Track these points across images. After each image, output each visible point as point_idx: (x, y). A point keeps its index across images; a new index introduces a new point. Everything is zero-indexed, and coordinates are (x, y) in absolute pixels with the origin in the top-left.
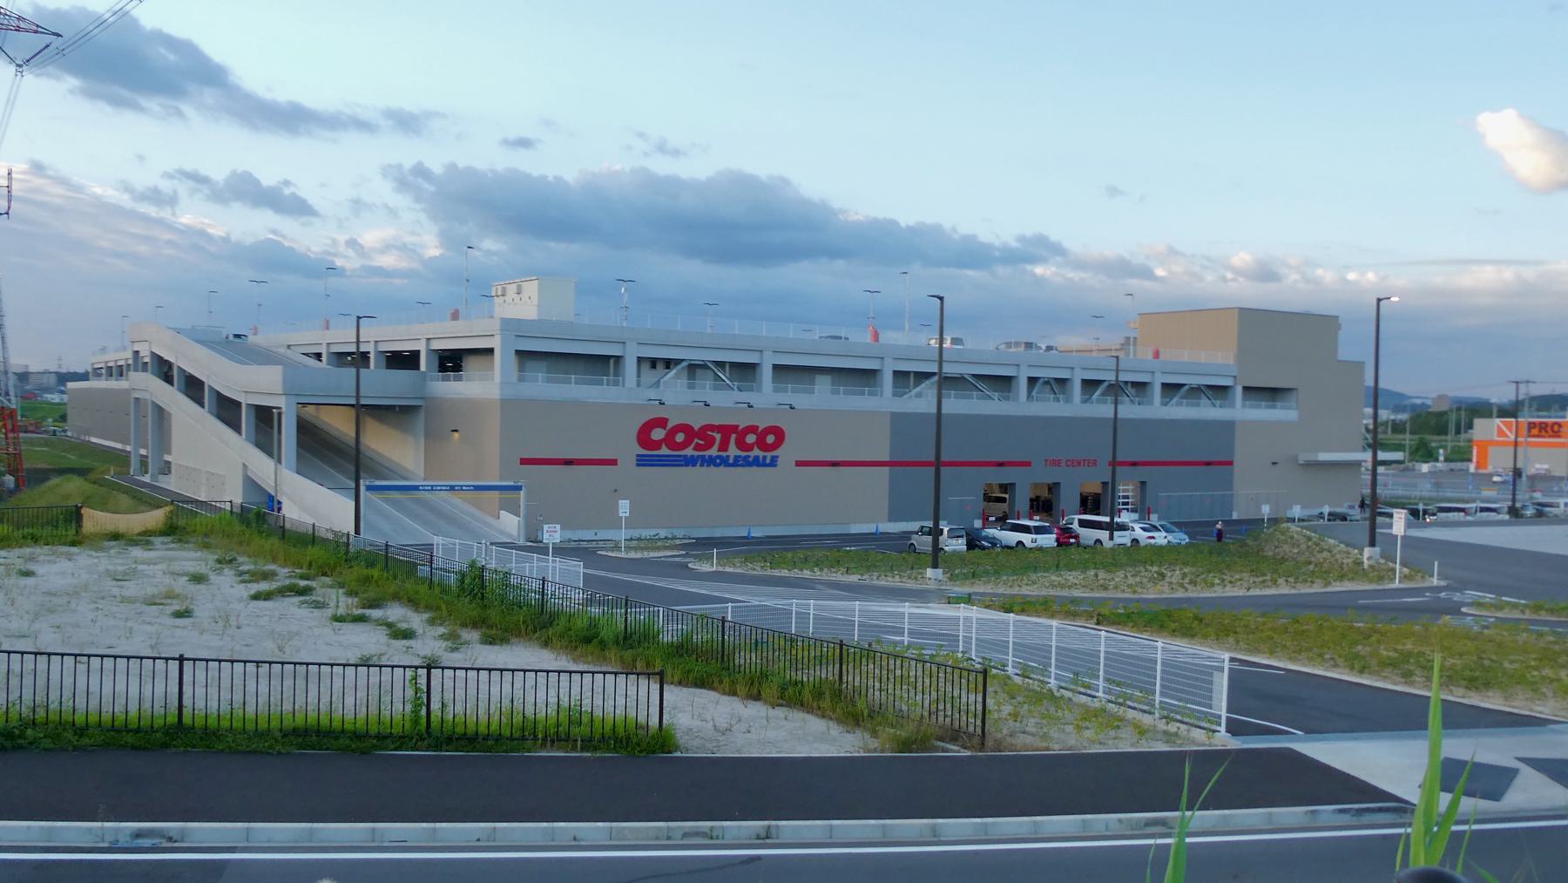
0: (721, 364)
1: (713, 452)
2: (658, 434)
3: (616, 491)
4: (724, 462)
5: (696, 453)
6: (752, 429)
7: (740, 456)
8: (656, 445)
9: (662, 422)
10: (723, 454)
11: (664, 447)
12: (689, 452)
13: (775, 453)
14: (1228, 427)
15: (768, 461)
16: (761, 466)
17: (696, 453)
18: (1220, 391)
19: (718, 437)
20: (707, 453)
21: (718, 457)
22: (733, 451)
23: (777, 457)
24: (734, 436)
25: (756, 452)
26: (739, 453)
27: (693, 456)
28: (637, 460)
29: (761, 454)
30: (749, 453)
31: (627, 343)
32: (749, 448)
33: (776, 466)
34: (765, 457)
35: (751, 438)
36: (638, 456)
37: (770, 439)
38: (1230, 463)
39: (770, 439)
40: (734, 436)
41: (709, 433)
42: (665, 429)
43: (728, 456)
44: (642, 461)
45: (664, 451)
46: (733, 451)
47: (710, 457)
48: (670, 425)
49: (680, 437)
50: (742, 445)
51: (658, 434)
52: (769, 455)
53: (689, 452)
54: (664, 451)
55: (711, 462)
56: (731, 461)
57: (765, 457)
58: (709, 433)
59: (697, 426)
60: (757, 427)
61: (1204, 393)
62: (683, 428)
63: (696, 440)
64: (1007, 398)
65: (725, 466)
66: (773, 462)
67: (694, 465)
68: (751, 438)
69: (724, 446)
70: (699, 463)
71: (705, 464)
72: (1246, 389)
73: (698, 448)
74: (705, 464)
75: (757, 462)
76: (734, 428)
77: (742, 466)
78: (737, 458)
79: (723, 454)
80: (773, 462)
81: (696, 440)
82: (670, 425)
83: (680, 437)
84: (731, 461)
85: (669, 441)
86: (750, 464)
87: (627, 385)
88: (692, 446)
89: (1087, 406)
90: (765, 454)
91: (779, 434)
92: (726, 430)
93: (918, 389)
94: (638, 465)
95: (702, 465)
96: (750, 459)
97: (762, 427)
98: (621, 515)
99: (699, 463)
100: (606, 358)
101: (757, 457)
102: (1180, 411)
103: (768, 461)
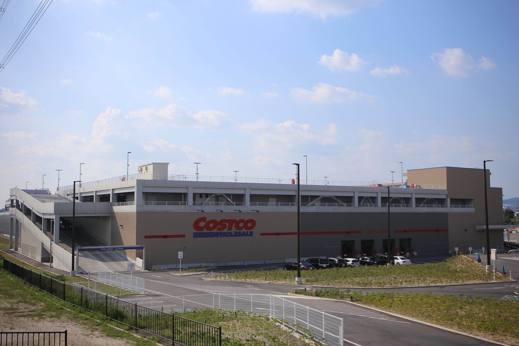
0: (229, 195)
1: (226, 231)
2: (202, 224)
3: (185, 248)
4: (230, 235)
6: (242, 221)
7: (237, 232)
8: (202, 228)
9: (204, 219)
10: (230, 231)
11: (205, 229)
12: (215, 231)
13: (252, 230)
14: (446, 215)
15: (249, 234)
16: (246, 236)
17: (218, 231)
18: (441, 202)
19: (227, 224)
20: (223, 231)
21: (227, 233)
22: (234, 230)
23: (253, 232)
24: (234, 224)
25: (244, 230)
26: (236, 231)
27: (217, 232)
28: (194, 235)
29: (246, 231)
30: (240, 231)
31: (189, 188)
32: (241, 228)
33: (252, 235)
34: (247, 232)
35: (241, 225)
36: (194, 233)
37: (250, 225)
38: (447, 230)
39: (250, 225)
40: (234, 224)
41: (224, 223)
42: (205, 222)
44: (195, 235)
45: (205, 231)
46: (234, 230)
48: (207, 220)
49: (211, 225)
50: (237, 227)
51: (202, 224)
52: (249, 231)
53: (215, 231)
54: (205, 231)
55: (225, 235)
56: (233, 234)
57: (247, 232)
58: (224, 223)
60: (244, 220)
61: (435, 202)
62: (213, 221)
63: (218, 226)
64: (350, 206)
65: (230, 236)
66: (251, 234)
67: (217, 236)
68: (241, 225)
69: (230, 228)
70: (219, 236)
71: (222, 236)
72: (451, 199)
73: (219, 229)
74: (222, 236)
75: (244, 234)
76: (234, 221)
77: (237, 236)
78: (235, 233)
79: (230, 231)
80: (251, 234)
81: (218, 226)
82: (207, 220)
83: (211, 225)
84: (233, 234)
85: (207, 226)
86: (241, 235)
87: (189, 205)
88: (216, 229)
89: (384, 208)
90: (247, 231)
91: (253, 222)
92: (231, 222)
93: (312, 203)
94: (194, 237)
95: (221, 236)
96: (241, 233)
97: (246, 219)
98: (179, 258)
99: (219, 236)
100: (181, 194)
101: (244, 232)
102: (424, 209)
103: (249, 234)
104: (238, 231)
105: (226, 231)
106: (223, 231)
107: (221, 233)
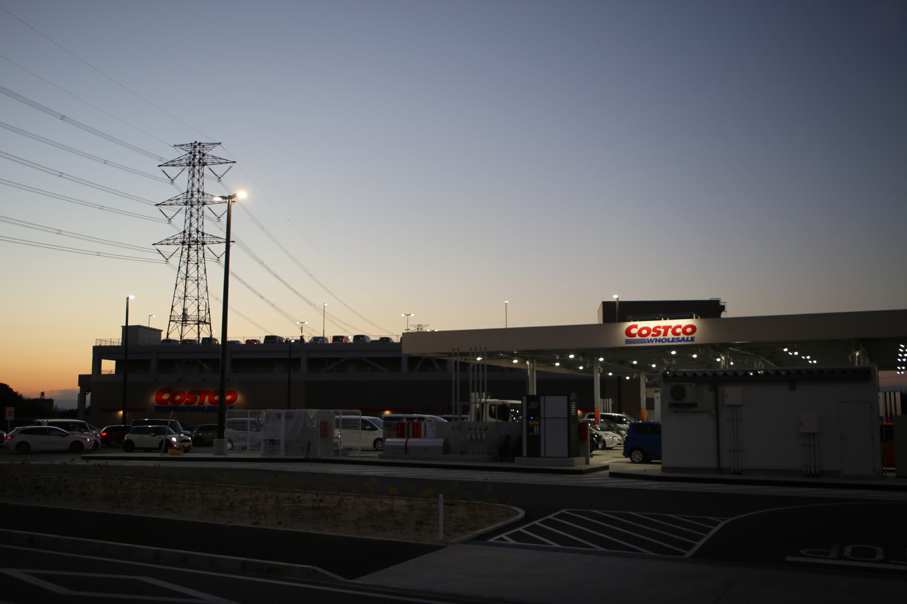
1: (661, 337)
5: (653, 338)
13: (692, 336)
15: (690, 339)
17: (653, 338)
20: (658, 338)
21: (663, 339)
23: (694, 337)
24: (670, 330)
29: (685, 337)
34: (688, 338)
40: (670, 330)
43: (669, 339)
47: (660, 339)
52: (690, 337)
54: (638, 337)
56: (671, 340)
57: (688, 338)
59: (652, 328)
73: (653, 335)
84: (671, 340)
90: (688, 336)
96: (680, 339)
101: (683, 338)
104: (676, 337)
105: (661, 337)
106: (658, 338)
107: (656, 339)
